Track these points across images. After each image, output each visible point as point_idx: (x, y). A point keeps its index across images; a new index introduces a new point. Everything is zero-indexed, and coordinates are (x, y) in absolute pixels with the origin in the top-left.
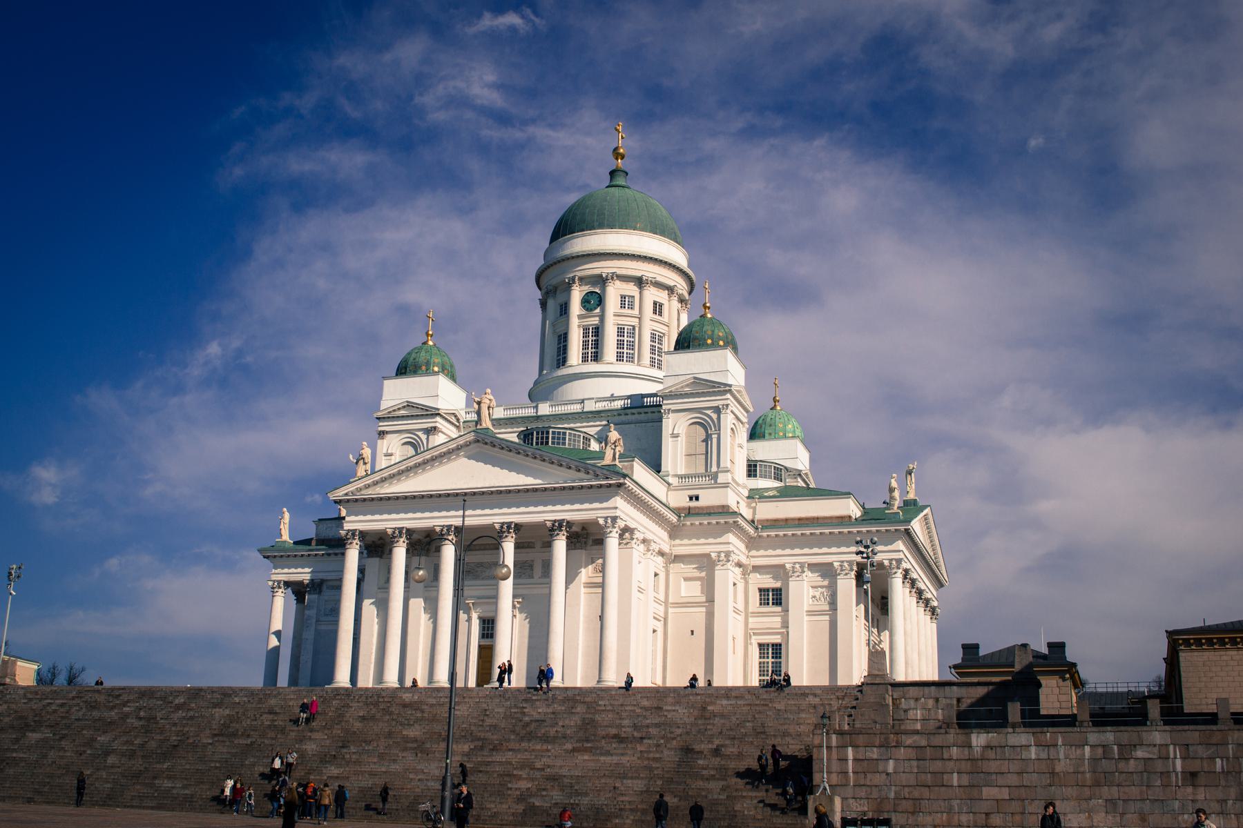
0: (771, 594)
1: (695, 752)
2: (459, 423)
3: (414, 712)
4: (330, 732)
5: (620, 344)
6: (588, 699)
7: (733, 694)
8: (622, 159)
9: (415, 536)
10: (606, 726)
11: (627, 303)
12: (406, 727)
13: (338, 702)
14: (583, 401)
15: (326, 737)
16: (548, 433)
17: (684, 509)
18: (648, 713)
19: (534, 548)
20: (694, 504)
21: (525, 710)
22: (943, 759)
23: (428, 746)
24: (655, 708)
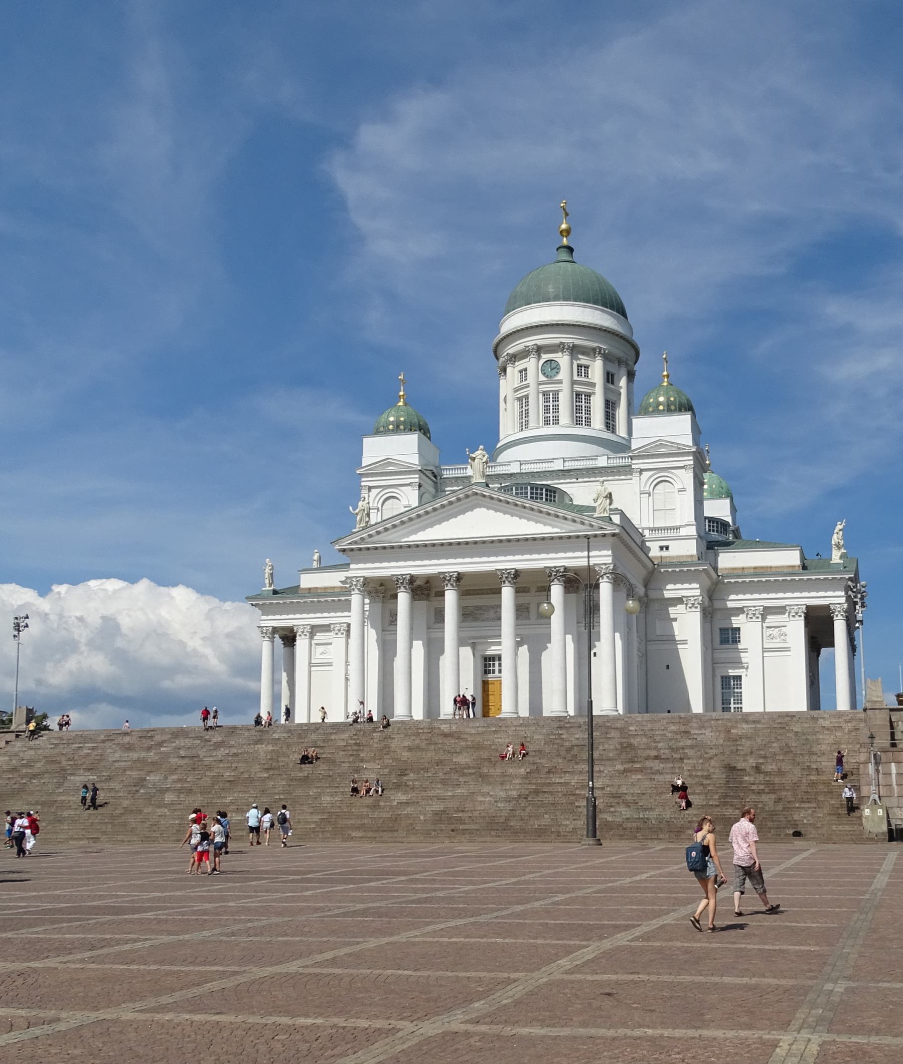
1: (738, 770)
2: (436, 479)
3: (457, 741)
4: (381, 761)
5: (578, 409)
6: (619, 725)
7: (750, 719)
9: (418, 583)
10: (645, 749)
11: (583, 371)
12: (455, 755)
13: (379, 734)
14: (551, 461)
15: (379, 767)
16: (526, 488)
17: (656, 558)
18: (679, 737)
19: (529, 592)
20: (665, 553)
21: (562, 736)
23: (486, 772)
24: (683, 732)
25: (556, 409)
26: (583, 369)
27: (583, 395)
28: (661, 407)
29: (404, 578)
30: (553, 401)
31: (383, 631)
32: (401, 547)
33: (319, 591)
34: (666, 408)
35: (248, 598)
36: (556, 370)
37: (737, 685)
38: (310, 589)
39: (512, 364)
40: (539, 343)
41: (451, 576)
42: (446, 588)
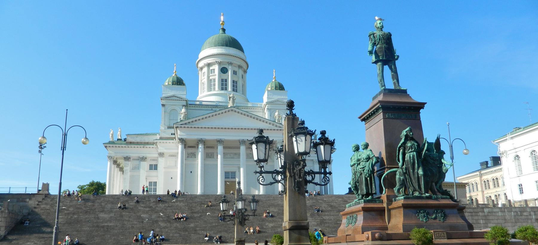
3: (262, 203)
22: (478, 216)
25: (226, 85)
34: (279, 88)
35: (103, 144)
40: (209, 62)
42: (218, 145)
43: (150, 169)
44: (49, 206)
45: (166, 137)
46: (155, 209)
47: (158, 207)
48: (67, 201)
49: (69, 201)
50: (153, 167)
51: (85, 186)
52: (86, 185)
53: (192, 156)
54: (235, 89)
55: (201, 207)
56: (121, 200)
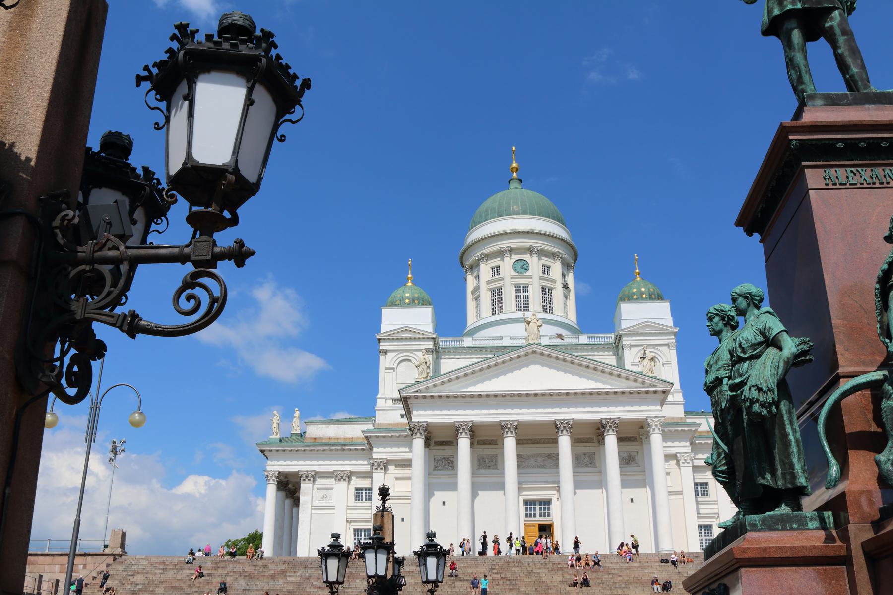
0: (699, 487)
3: (611, 576)
5: (544, 300)
8: (516, 172)
25: (526, 298)
26: (546, 269)
27: (547, 289)
28: (644, 296)
29: (466, 425)
30: (523, 292)
31: (429, 475)
32: (464, 396)
33: (324, 441)
34: (648, 297)
36: (525, 267)
37: (708, 532)
38: (315, 439)
39: (485, 262)
41: (512, 424)
42: (505, 436)
43: (356, 500)
44: (116, 582)
45: (390, 424)
46: (344, 592)
47: (351, 587)
48: (156, 571)
49: (161, 571)
50: (364, 497)
51: (239, 542)
52: (242, 540)
53: (446, 465)
54: (547, 305)
55: (454, 587)
56: (269, 570)
